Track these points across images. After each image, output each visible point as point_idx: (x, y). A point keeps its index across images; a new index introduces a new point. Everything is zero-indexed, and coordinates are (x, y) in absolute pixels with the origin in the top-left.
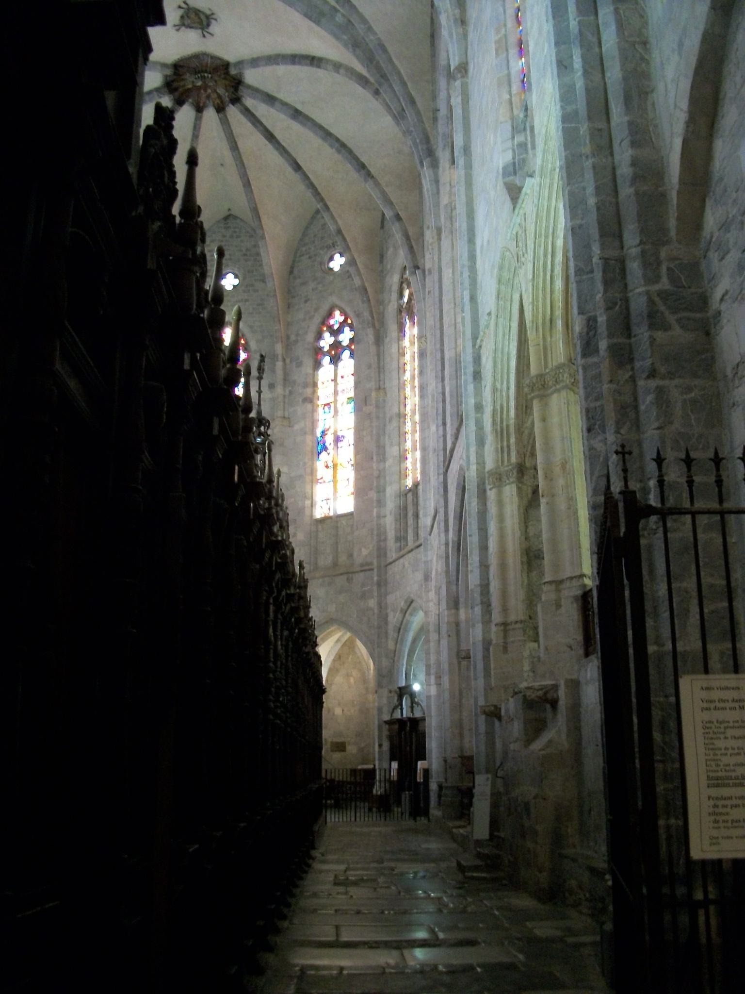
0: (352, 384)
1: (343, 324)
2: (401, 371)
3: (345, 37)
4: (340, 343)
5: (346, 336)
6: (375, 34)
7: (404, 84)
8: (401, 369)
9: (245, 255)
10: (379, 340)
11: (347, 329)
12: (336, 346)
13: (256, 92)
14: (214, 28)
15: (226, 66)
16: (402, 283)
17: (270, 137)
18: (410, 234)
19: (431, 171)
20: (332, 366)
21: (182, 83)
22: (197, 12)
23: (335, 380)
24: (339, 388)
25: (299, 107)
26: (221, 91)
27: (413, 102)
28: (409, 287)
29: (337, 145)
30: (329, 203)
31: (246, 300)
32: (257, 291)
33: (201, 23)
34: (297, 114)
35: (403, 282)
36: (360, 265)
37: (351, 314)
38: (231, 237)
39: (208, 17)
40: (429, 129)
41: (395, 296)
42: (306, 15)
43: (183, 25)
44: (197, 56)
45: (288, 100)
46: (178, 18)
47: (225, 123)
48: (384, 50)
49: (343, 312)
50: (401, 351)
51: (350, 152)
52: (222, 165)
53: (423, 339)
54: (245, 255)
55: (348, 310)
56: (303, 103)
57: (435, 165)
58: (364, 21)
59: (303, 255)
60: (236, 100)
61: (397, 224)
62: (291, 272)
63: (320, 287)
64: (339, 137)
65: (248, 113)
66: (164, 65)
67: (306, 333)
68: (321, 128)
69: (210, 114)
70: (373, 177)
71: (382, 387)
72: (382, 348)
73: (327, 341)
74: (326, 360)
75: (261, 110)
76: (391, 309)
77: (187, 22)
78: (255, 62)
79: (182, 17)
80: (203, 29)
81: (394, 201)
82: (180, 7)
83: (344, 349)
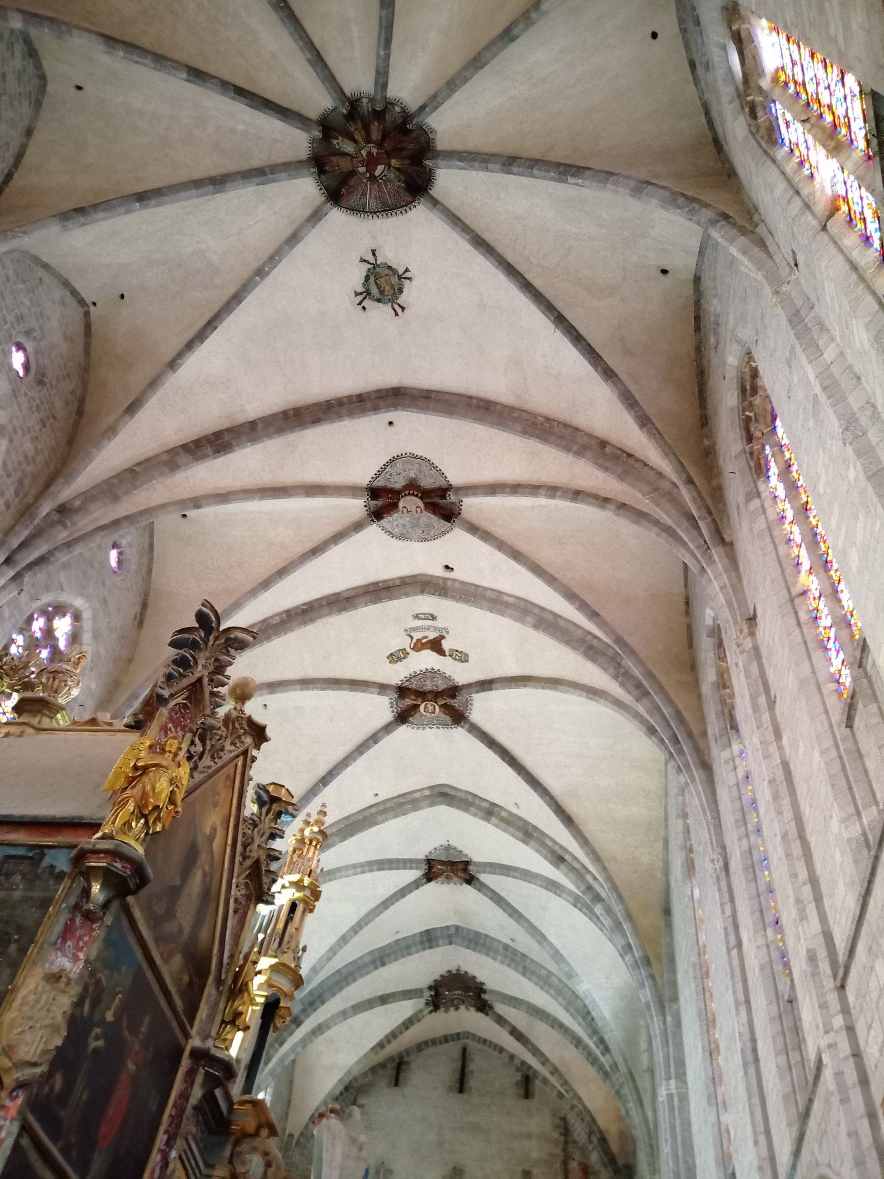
14: (356, 276)
33: (377, 277)
39: (368, 293)
46: (405, 290)
77: (394, 280)
79: (401, 291)
80: (375, 266)
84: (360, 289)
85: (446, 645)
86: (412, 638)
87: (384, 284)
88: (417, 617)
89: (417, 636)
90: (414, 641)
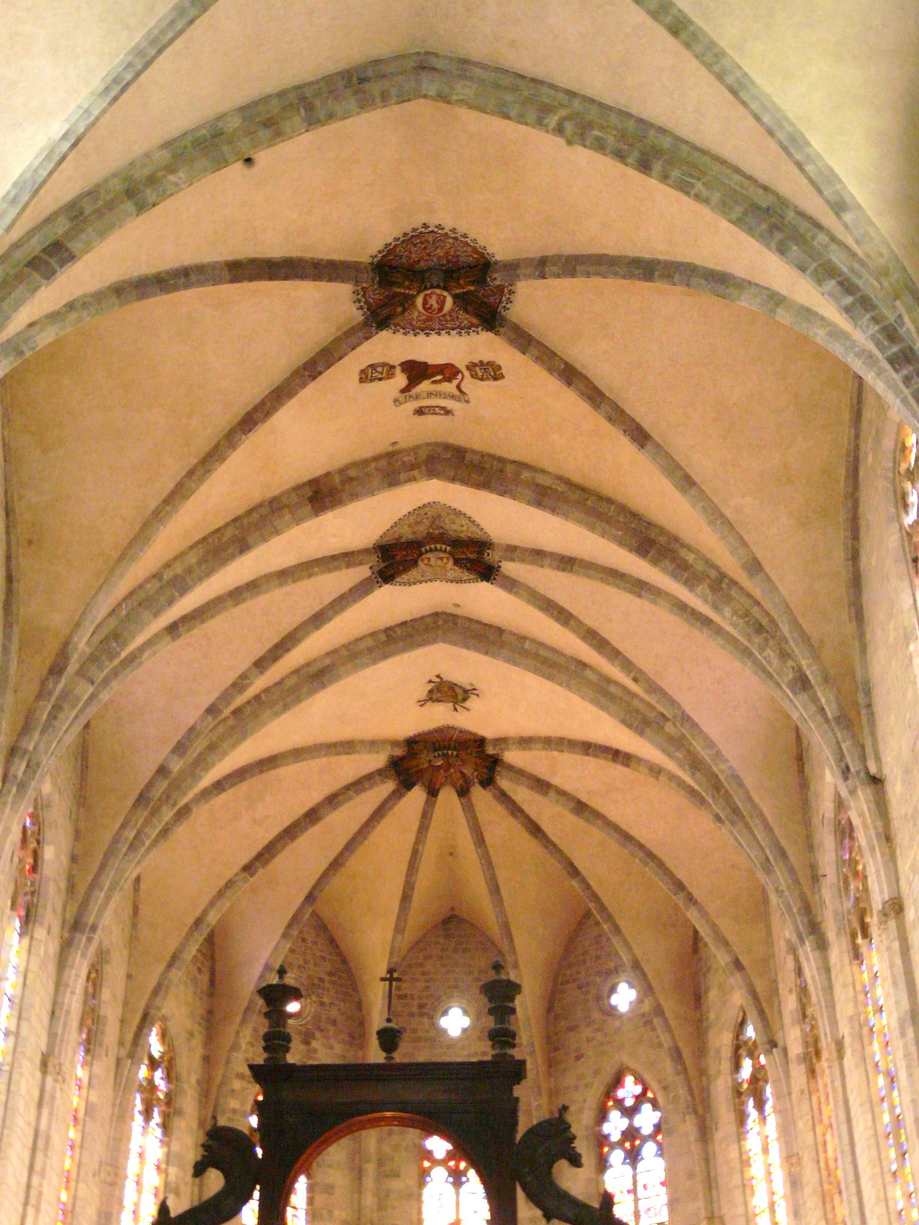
0: (664, 1199)
1: (640, 1099)
2: (748, 1191)
3: (677, 754)
4: (637, 1130)
5: (647, 1119)
6: (726, 761)
7: (768, 828)
8: (746, 1187)
10: (705, 1133)
11: (647, 1108)
12: (631, 1134)
13: (520, 774)
15: (481, 742)
16: (737, 1048)
17: (535, 830)
18: (758, 990)
19: (817, 953)
20: (628, 1169)
21: (414, 763)
22: (452, 686)
23: (634, 1191)
24: (642, 1206)
25: (584, 798)
26: (467, 771)
27: (783, 855)
28: (751, 1055)
29: (641, 854)
30: (621, 923)
34: (581, 808)
35: (739, 1049)
36: (668, 1014)
37: (654, 1084)
38: (455, 951)
39: (466, 691)
40: (809, 894)
41: (726, 1065)
42: (623, 722)
43: (431, 699)
44: (439, 730)
45: (567, 788)
47: (469, 809)
48: (741, 785)
49: (639, 1080)
50: (745, 1157)
51: (661, 865)
52: (451, 854)
53: (794, 1160)
55: (647, 1077)
56: (589, 793)
57: (822, 945)
58: (711, 744)
59: (568, 982)
60: (488, 782)
61: (738, 976)
62: (550, 1009)
63: (599, 1036)
64: (643, 841)
65: (504, 798)
66: (395, 743)
67: (581, 1110)
68: (616, 828)
69: (448, 797)
70: (695, 903)
71: (716, 1213)
72: (710, 1148)
73: (615, 1125)
74: (617, 1157)
75: (522, 795)
76: (721, 1089)
78: (525, 742)
79: (431, 691)
80: (455, 703)
81: (730, 938)
82: (430, 681)
83: (645, 1139)
84: (473, 697)
85: (401, 380)
86: (458, 387)
87: (449, 693)
88: (447, 412)
89: (449, 387)
90: (455, 382)
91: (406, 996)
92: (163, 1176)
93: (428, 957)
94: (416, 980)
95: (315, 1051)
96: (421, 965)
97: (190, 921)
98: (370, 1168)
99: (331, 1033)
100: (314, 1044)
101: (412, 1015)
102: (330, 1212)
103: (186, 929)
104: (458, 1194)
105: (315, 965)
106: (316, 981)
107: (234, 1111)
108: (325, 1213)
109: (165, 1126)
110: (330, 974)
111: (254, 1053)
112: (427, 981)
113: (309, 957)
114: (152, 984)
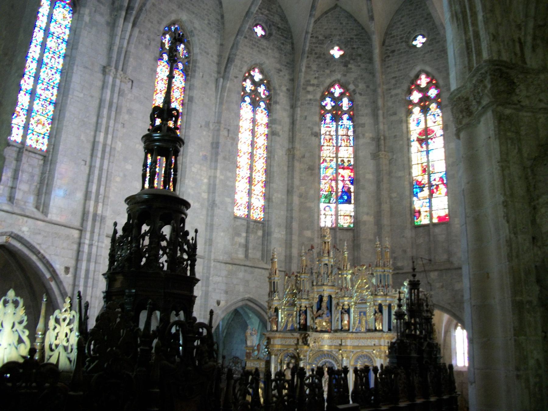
9: (426, 19)
31: (432, 51)
32: (439, 42)
38: (415, 9)
54: (426, 19)
91: (394, 36)
92: (270, 129)
93: (402, 17)
94: (399, 28)
95: (351, 68)
96: (400, 21)
97: (244, 14)
98: (380, 112)
99: (359, 60)
100: (350, 66)
101: (397, 43)
102: (363, 135)
103: (243, 18)
104: (426, 116)
105: (348, 32)
106: (349, 39)
107: (310, 100)
108: (361, 135)
109: (269, 108)
110: (356, 35)
111: (319, 74)
112: (404, 27)
113: (344, 30)
114: (230, 45)
